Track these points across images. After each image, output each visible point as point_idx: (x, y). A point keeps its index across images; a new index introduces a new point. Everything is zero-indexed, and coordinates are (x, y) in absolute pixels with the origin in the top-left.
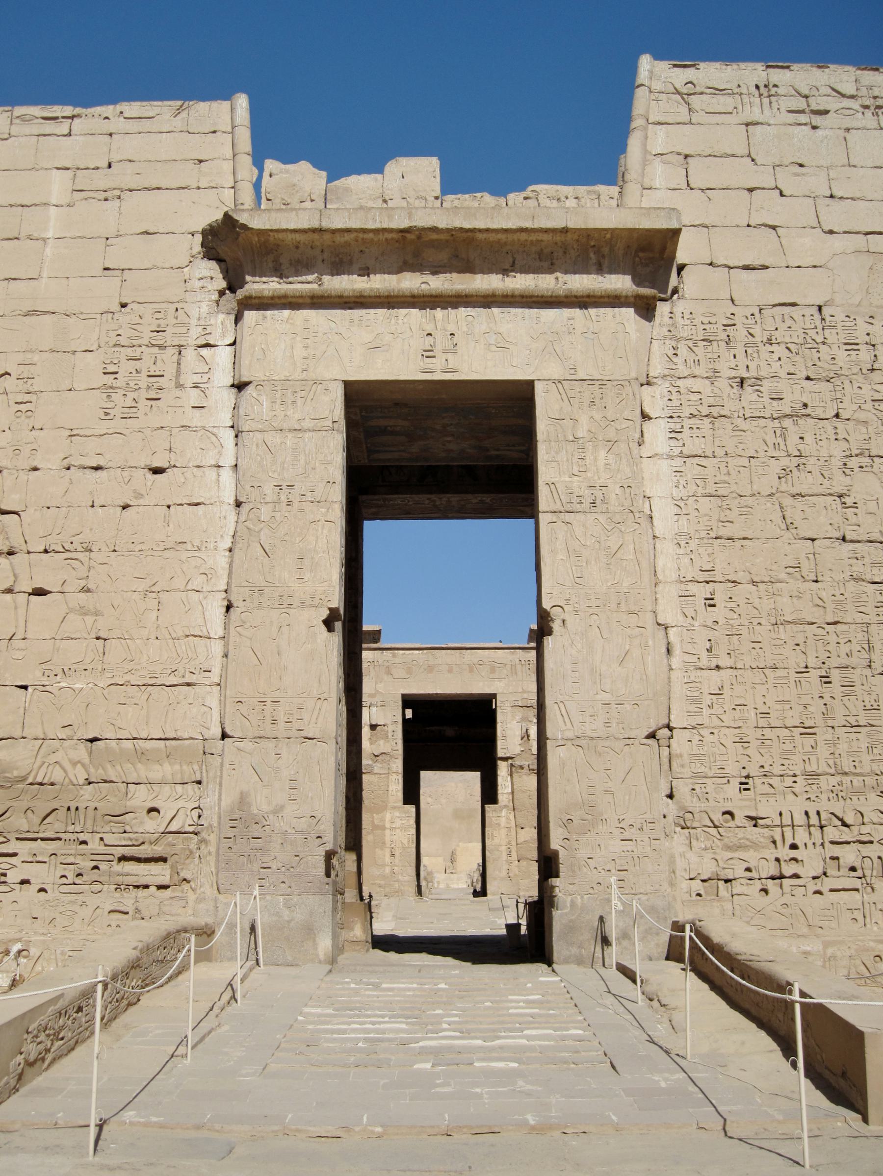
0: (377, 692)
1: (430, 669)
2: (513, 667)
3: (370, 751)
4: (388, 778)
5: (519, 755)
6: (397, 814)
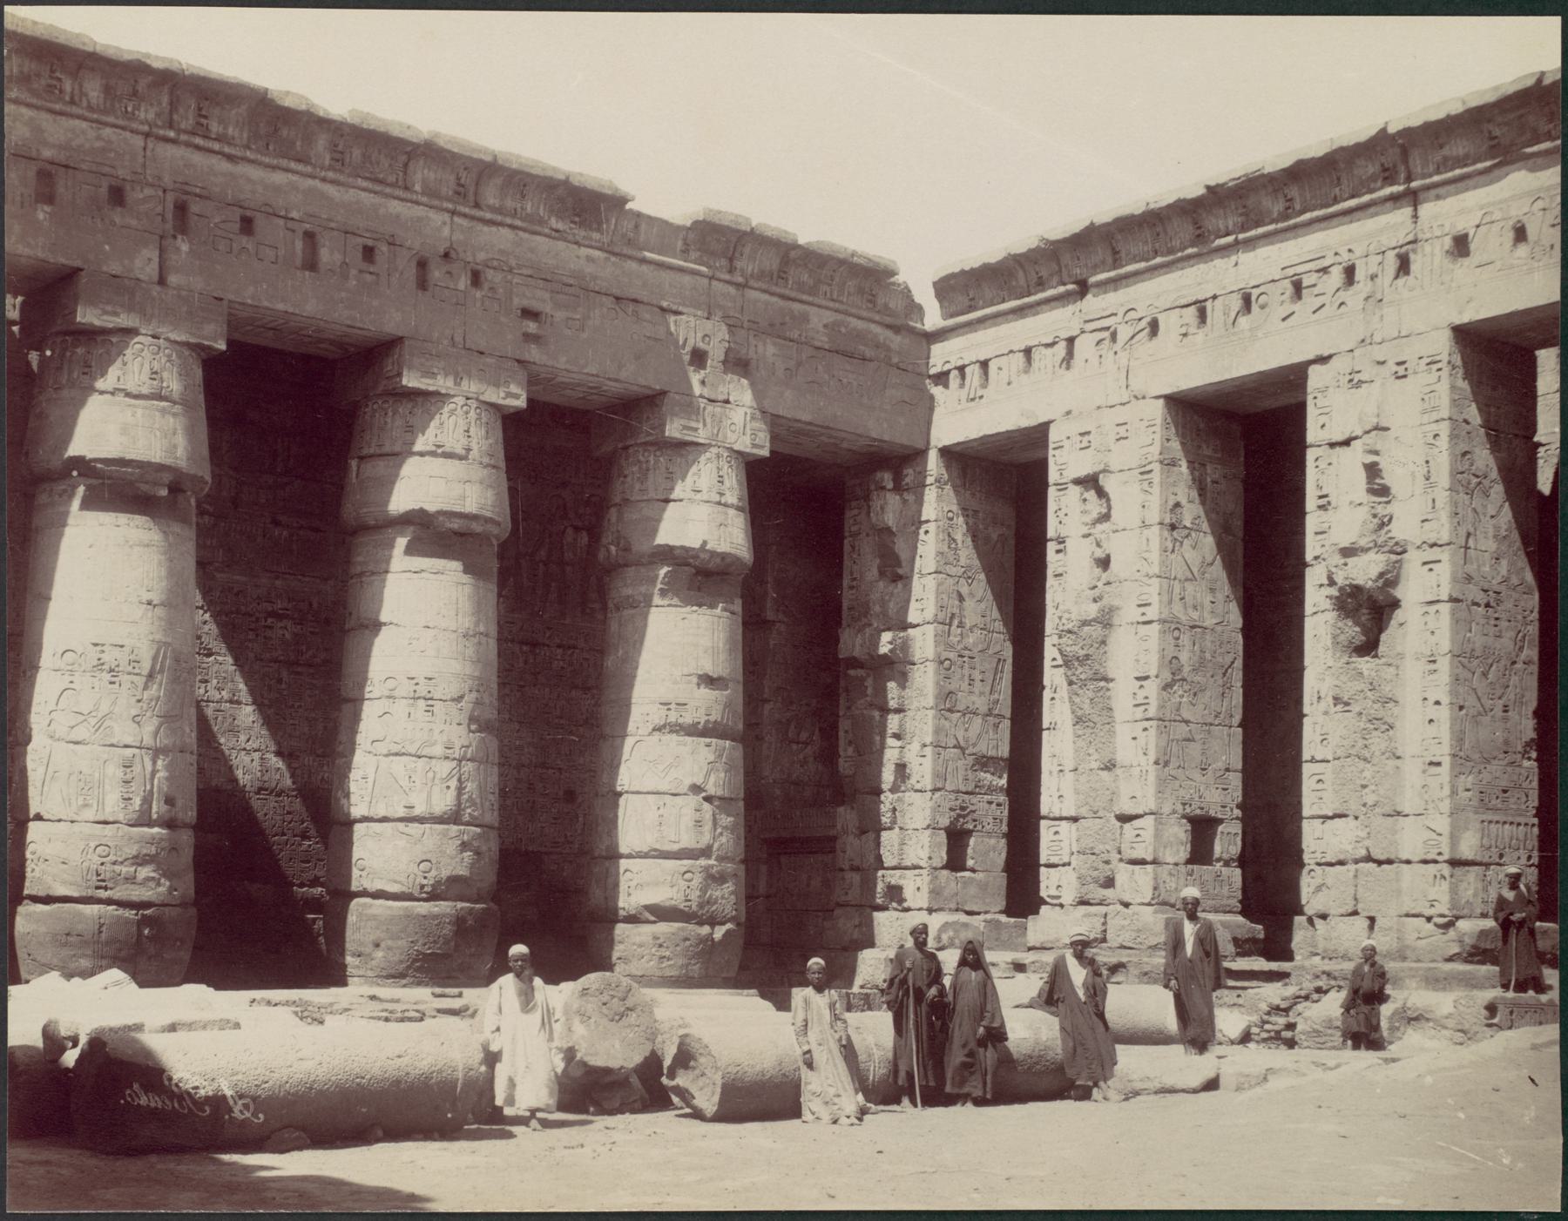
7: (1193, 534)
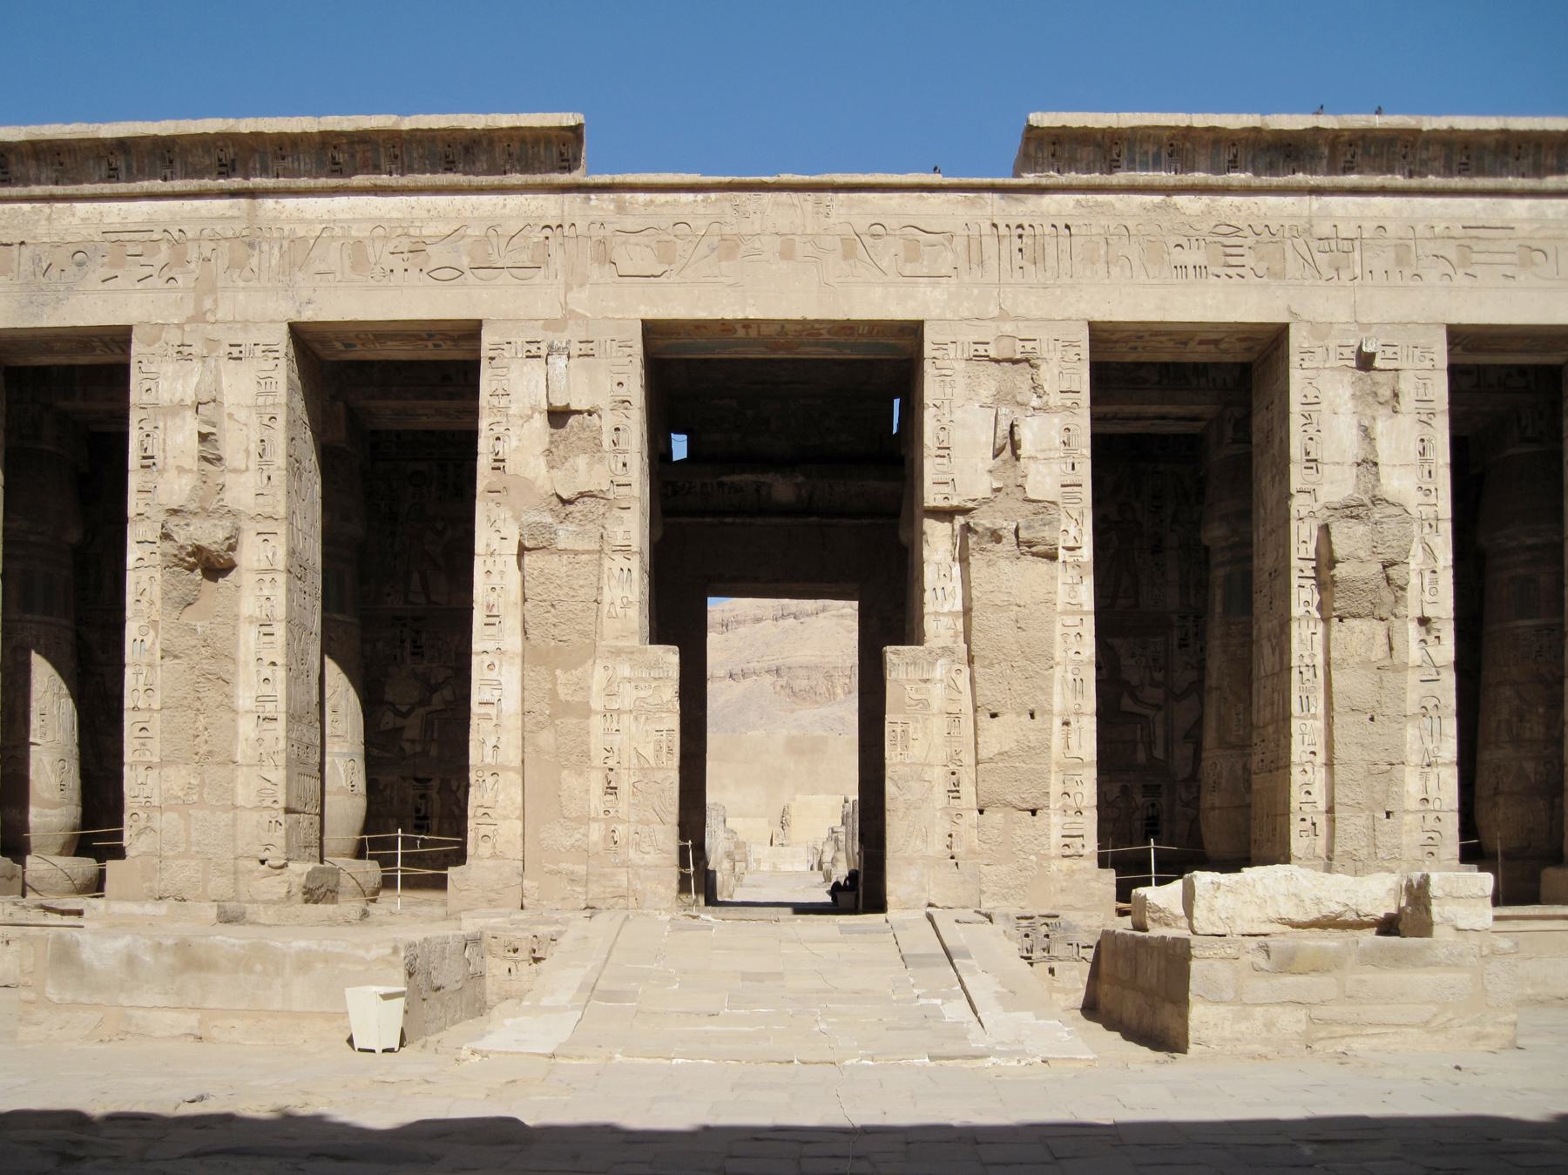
0: (569, 315)
1: (729, 247)
2: (974, 246)
3: (548, 488)
4: (601, 565)
5: (986, 501)
6: (625, 670)
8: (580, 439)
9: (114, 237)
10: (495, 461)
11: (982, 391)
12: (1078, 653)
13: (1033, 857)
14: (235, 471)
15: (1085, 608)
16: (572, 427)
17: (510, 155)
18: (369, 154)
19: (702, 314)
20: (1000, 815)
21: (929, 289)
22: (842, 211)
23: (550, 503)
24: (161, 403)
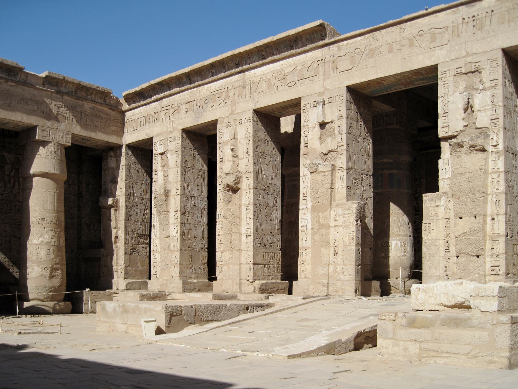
0: (325, 89)
1: (372, 53)
3: (320, 150)
5: (462, 131)
6: (340, 211)
7: (191, 169)
8: (329, 132)
9: (213, 93)
10: (306, 144)
11: (460, 87)
12: (498, 189)
13: (477, 275)
14: (241, 159)
15: (501, 170)
16: (327, 128)
17: (307, 40)
18: (270, 51)
19: (364, 80)
20: (465, 258)
21: (439, 51)
22: (409, 29)
23: (321, 156)
24: (225, 141)
